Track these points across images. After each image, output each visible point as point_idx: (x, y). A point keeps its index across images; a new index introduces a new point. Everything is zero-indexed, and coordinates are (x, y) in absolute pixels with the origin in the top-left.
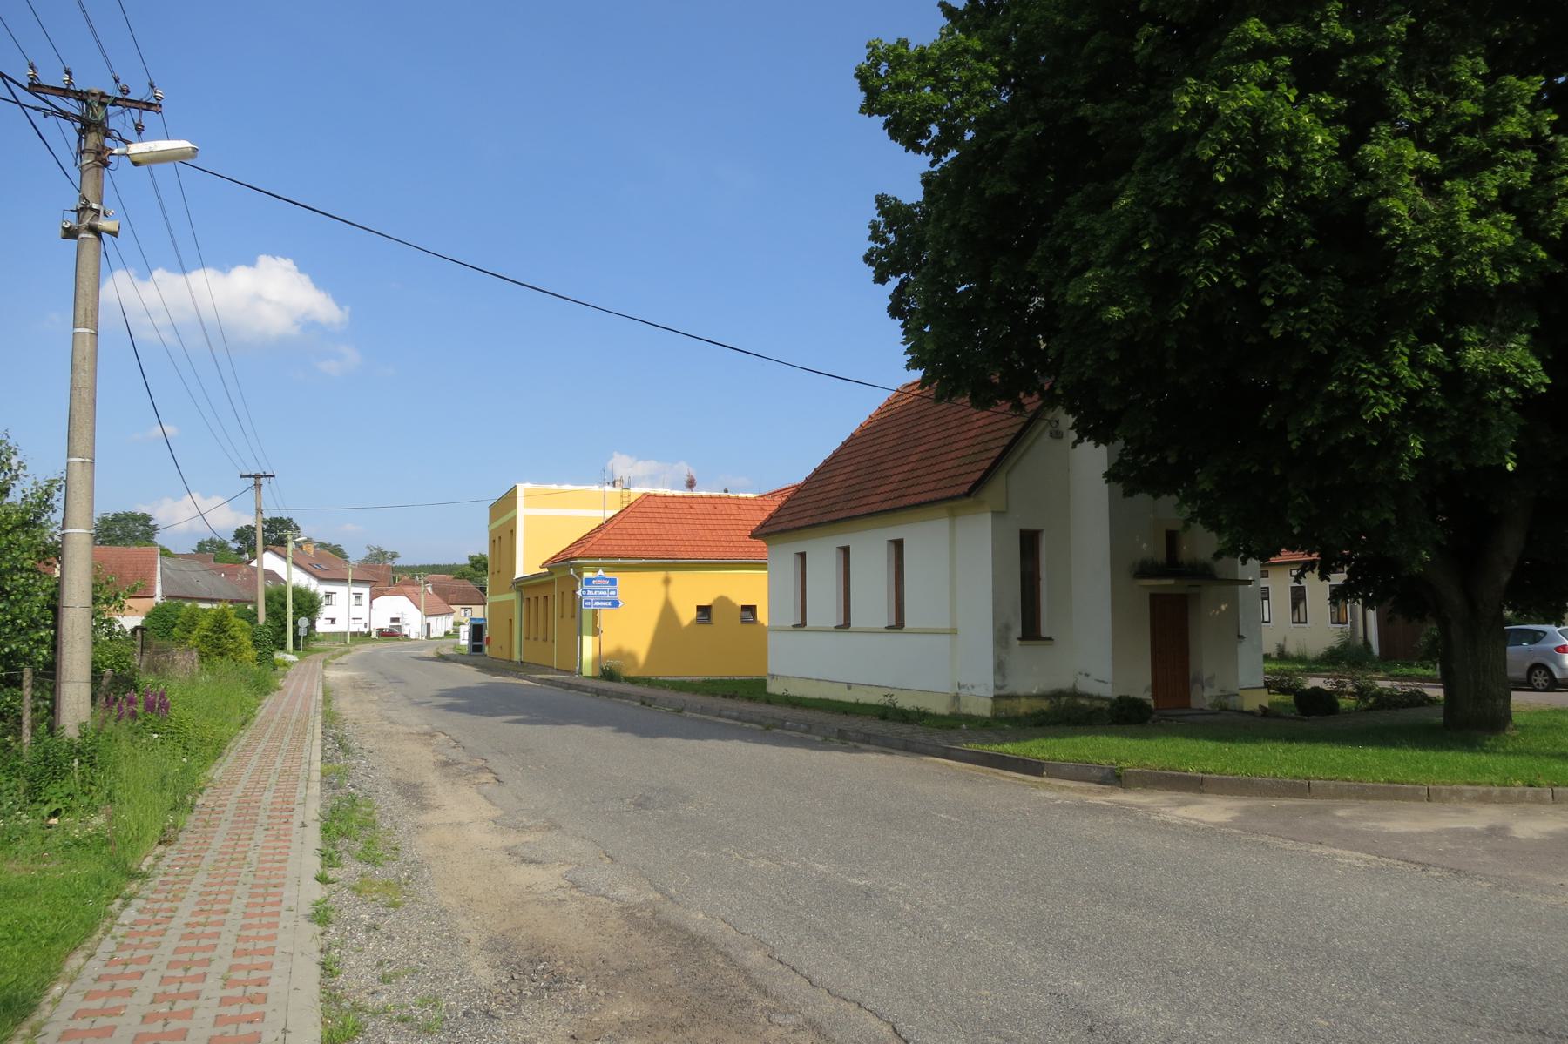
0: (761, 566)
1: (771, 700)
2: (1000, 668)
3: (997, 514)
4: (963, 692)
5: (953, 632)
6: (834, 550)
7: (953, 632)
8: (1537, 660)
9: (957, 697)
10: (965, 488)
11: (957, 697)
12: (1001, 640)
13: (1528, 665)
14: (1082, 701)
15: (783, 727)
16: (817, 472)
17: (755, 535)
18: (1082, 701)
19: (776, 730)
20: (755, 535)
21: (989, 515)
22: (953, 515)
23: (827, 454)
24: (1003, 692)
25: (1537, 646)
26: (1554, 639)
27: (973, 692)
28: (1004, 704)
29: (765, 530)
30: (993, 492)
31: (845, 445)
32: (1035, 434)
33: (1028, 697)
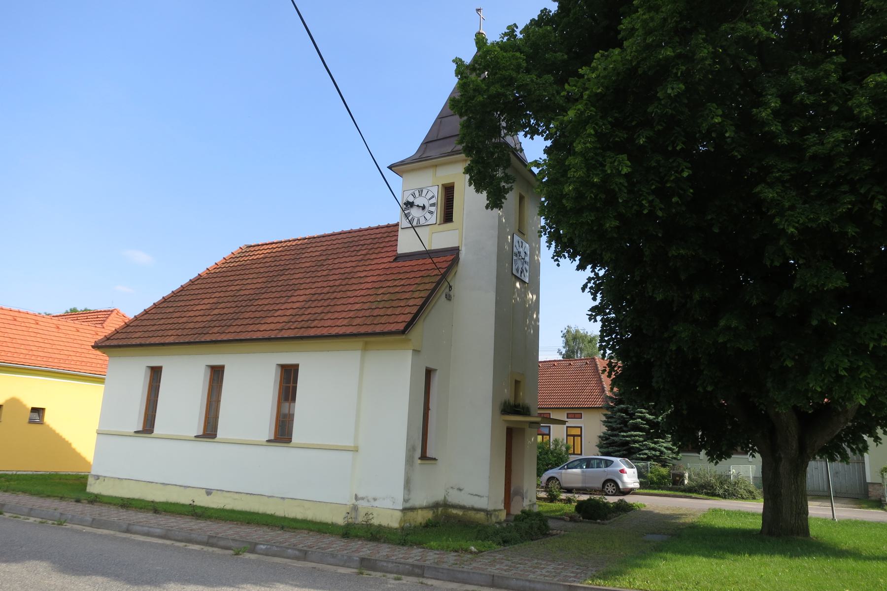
0: (98, 379)
1: (95, 499)
2: (408, 484)
3: (416, 352)
4: (360, 503)
5: (355, 450)
6: (275, 366)
7: (355, 450)
8: (609, 477)
9: (355, 508)
10: (401, 327)
11: (355, 508)
12: (409, 461)
13: (603, 480)
14: (455, 511)
15: (252, 551)
16: (165, 300)
17: (96, 346)
18: (455, 511)
19: (69, 526)
20: (96, 346)
21: (411, 352)
22: (365, 349)
23: (176, 287)
24: (408, 505)
25: (609, 469)
26: (618, 466)
27: (376, 504)
28: (410, 514)
29: (107, 343)
30: (416, 332)
31: (192, 282)
32: (438, 296)
33: (422, 508)
